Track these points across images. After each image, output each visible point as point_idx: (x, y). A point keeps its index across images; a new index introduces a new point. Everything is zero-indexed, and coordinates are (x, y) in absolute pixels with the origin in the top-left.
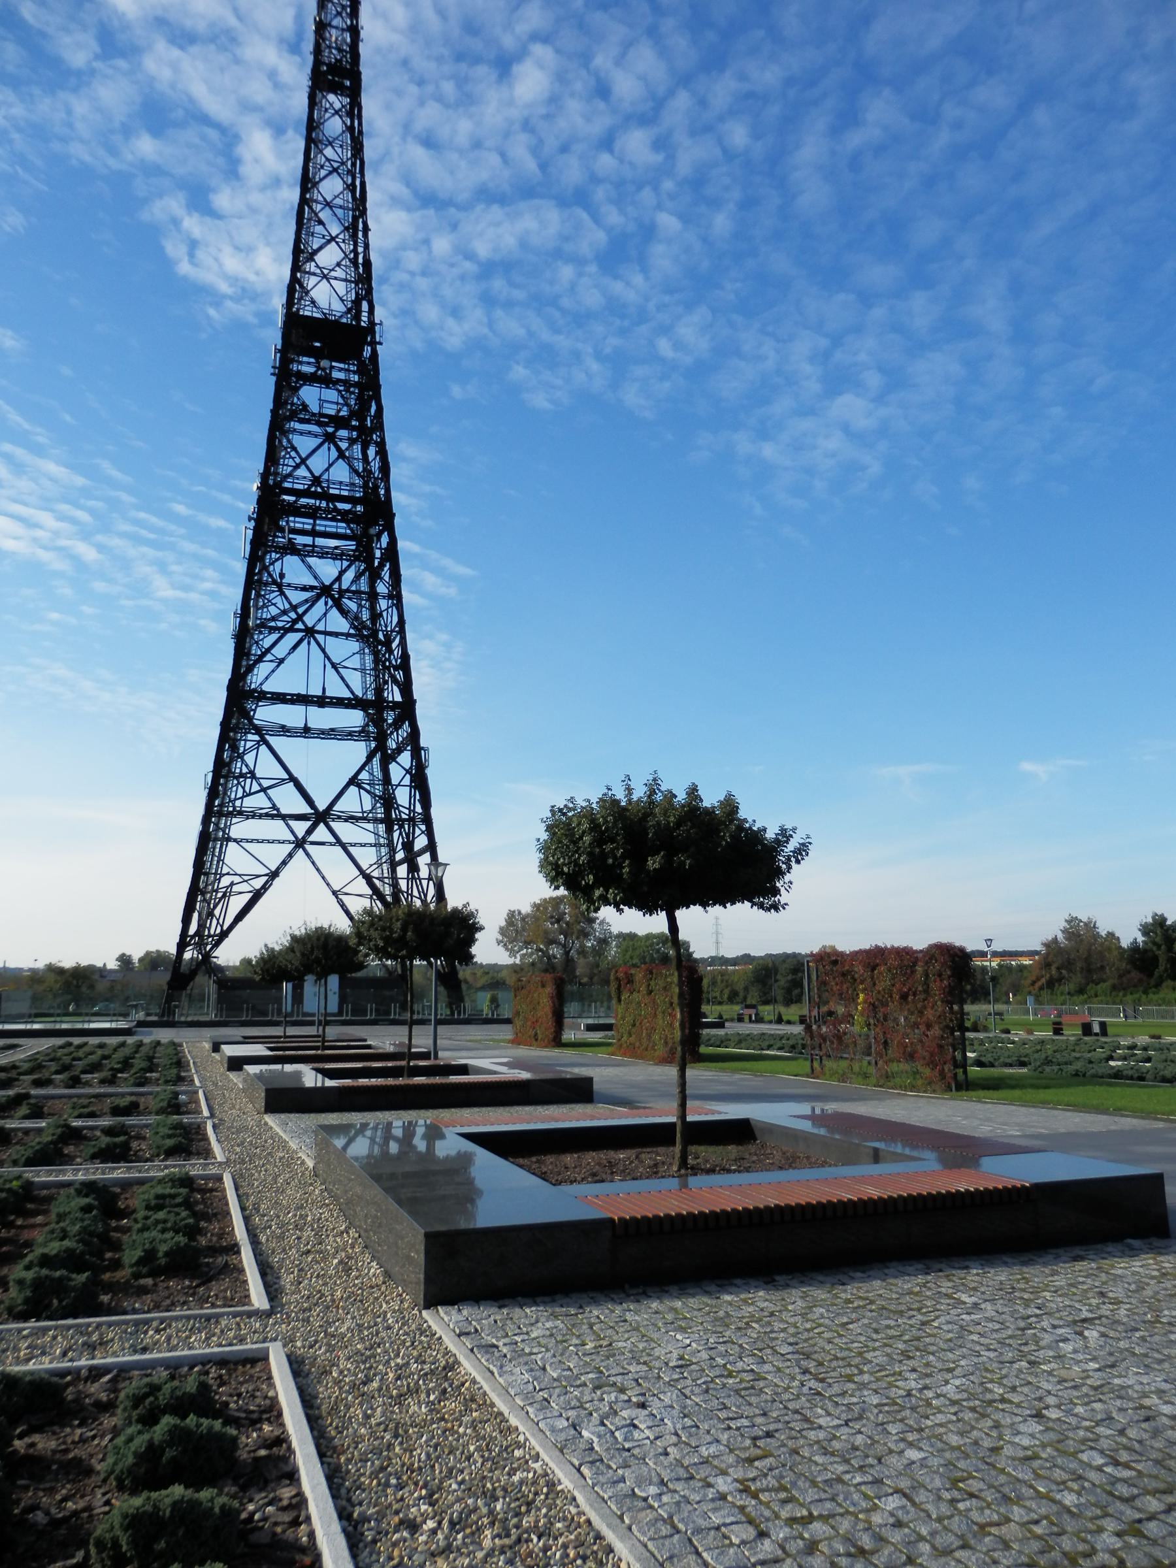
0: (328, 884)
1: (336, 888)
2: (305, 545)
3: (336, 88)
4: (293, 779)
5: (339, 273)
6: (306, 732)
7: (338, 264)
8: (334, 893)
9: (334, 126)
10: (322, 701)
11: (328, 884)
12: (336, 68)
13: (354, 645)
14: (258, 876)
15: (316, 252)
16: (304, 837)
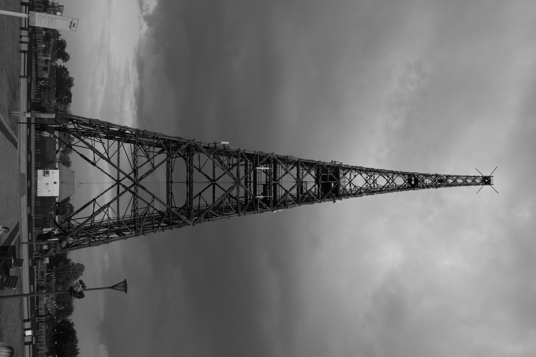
0: (98, 197)
1: (97, 200)
2: (250, 179)
3: (410, 181)
4: (154, 168)
5: (353, 187)
6: (169, 182)
7: (355, 187)
8: (94, 200)
9: (400, 181)
10: (189, 183)
11: (98, 197)
12: (416, 181)
13: (210, 202)
14: (108, 154)
15: (361, 175)
16: (121, 184)
